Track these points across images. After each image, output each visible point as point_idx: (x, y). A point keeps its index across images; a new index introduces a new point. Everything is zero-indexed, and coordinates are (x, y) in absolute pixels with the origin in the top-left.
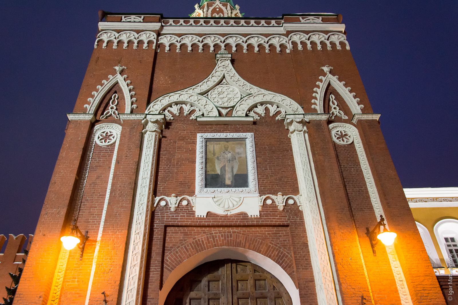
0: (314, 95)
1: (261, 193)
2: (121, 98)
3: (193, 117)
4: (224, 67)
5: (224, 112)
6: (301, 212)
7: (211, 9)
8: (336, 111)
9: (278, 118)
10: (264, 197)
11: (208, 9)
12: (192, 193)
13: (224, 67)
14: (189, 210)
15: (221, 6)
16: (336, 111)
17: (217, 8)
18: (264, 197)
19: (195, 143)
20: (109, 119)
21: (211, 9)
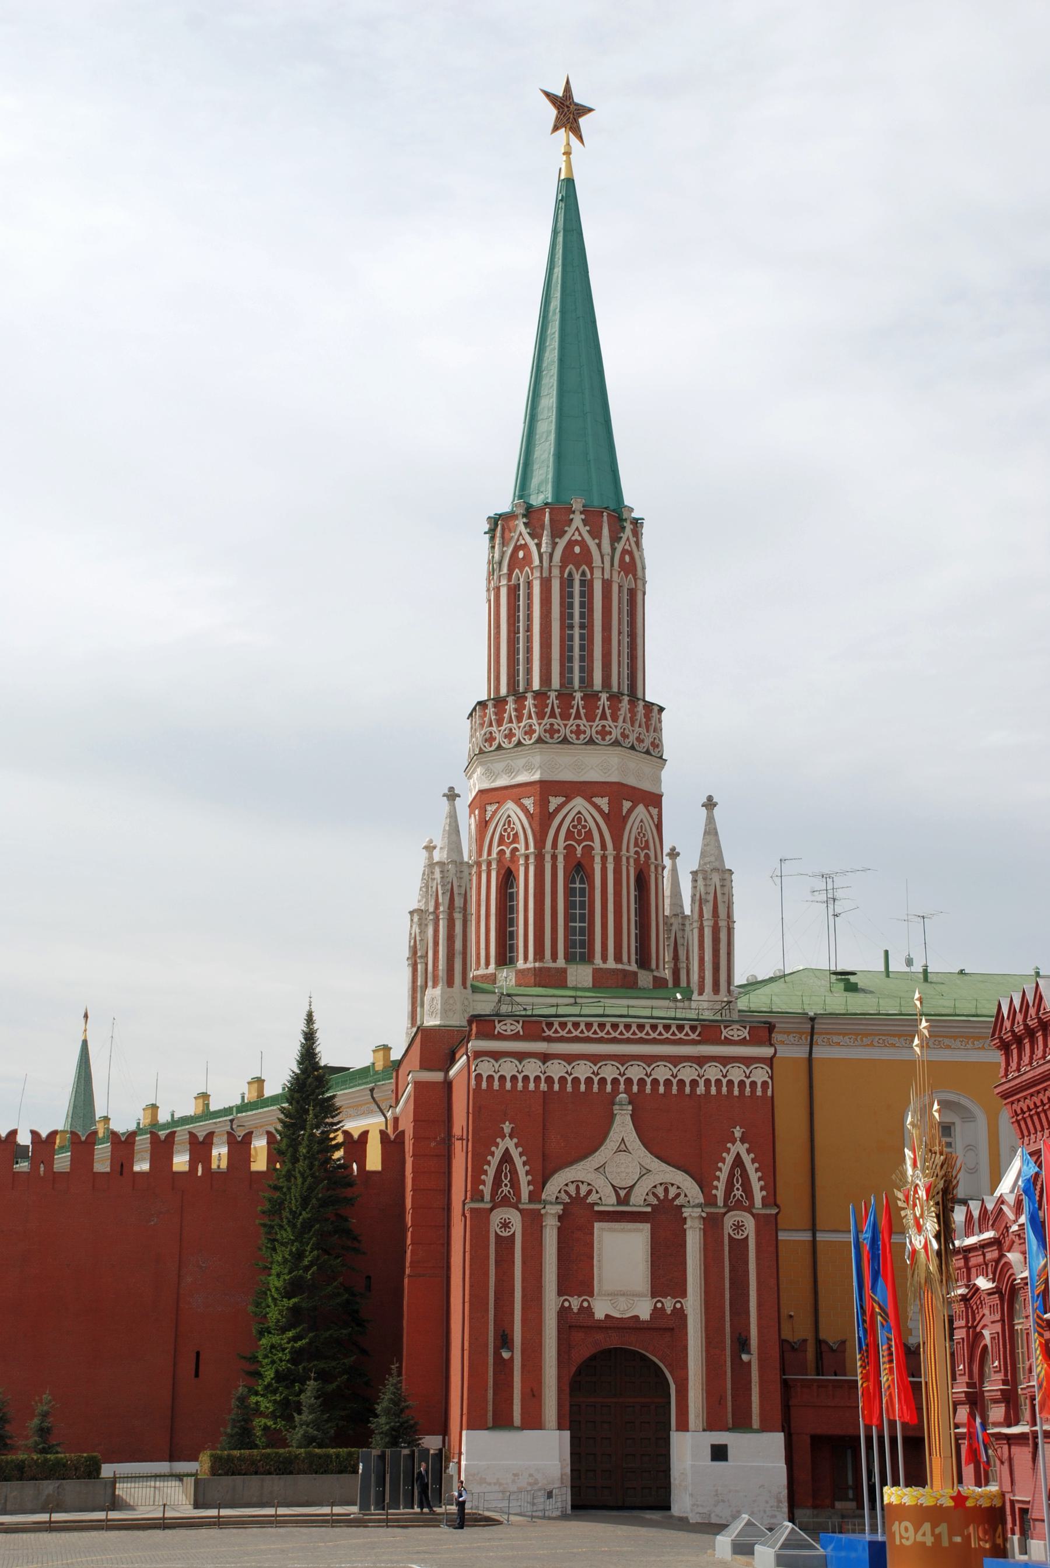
0: (718, 1173)
1: (653, 1296)
2: (514, 1172)
3: (589, 1200)
4: (623, 1127)
5: (622, 1193)
6: (686, 1316)
7: (562, 543)
8: (738, 1193)
9: (677, 1202)
10: (655, 1300)
11: (554, 545)
12: (591, 1294)
13: (623, 1127)
14: (588, 1311)
15: (584, 530)
16: (738, 1193)
17: (576, 542)
18: (655, 1300)
19: (592, 1234)
20: (505, 1202)
21: (562, 543)
